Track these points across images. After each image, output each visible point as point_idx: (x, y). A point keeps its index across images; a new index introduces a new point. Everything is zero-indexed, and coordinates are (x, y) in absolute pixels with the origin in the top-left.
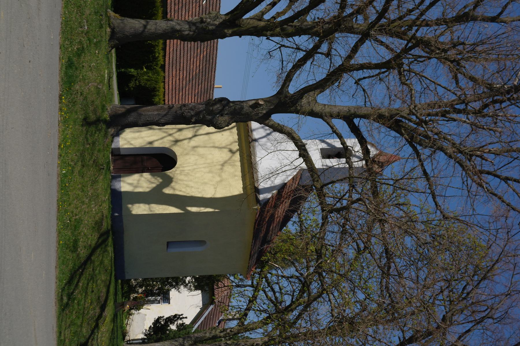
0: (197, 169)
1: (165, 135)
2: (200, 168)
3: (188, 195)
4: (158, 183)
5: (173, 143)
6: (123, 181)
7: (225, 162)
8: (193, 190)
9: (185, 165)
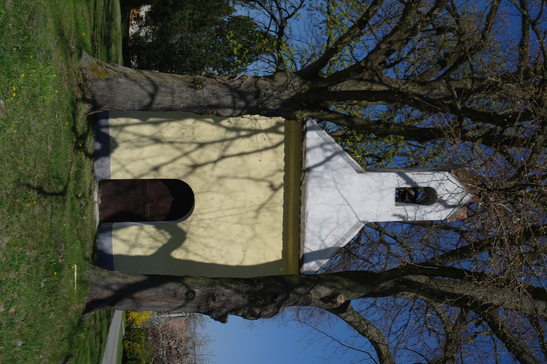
1: (178, 153)
2: (226, 216)
3: (206, 261)
4: (165, 242)
5: (189, 170)
6: (116, 237)
7: (262, 206)
8: (214, 253)
9: (205, 211)
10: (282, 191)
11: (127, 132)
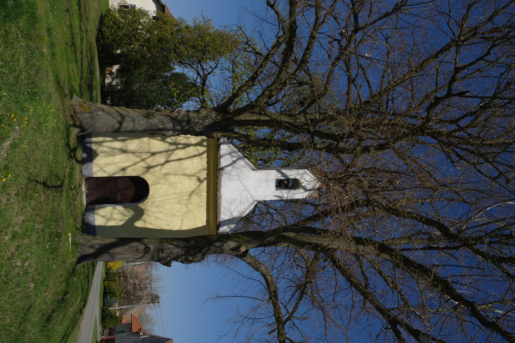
0: (167, 200)
1: (138, 159)
3: (157, 228)
4: (130, 216)
5: (145, 170)
6: (98, 214)
7: (193, 192)
8: (163, 222)
10: (205, 183)
11: (104, 146)
